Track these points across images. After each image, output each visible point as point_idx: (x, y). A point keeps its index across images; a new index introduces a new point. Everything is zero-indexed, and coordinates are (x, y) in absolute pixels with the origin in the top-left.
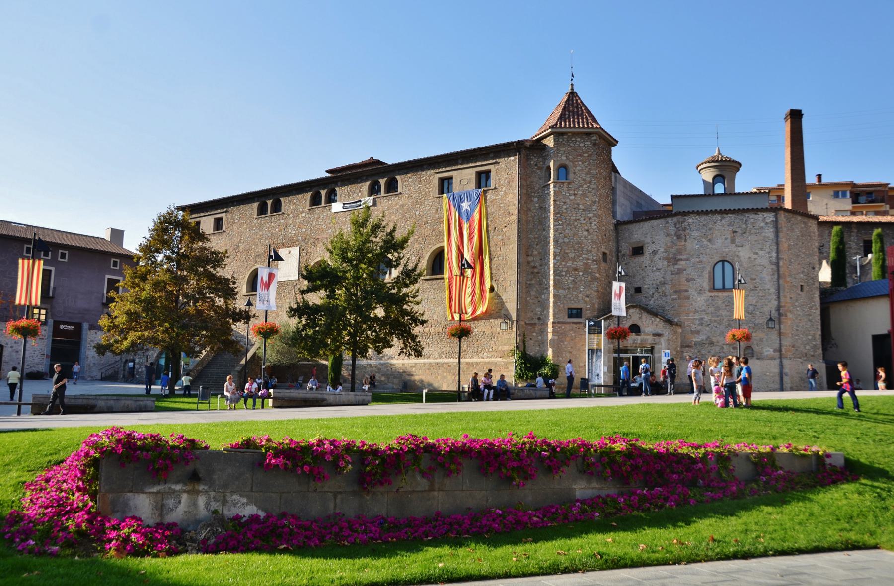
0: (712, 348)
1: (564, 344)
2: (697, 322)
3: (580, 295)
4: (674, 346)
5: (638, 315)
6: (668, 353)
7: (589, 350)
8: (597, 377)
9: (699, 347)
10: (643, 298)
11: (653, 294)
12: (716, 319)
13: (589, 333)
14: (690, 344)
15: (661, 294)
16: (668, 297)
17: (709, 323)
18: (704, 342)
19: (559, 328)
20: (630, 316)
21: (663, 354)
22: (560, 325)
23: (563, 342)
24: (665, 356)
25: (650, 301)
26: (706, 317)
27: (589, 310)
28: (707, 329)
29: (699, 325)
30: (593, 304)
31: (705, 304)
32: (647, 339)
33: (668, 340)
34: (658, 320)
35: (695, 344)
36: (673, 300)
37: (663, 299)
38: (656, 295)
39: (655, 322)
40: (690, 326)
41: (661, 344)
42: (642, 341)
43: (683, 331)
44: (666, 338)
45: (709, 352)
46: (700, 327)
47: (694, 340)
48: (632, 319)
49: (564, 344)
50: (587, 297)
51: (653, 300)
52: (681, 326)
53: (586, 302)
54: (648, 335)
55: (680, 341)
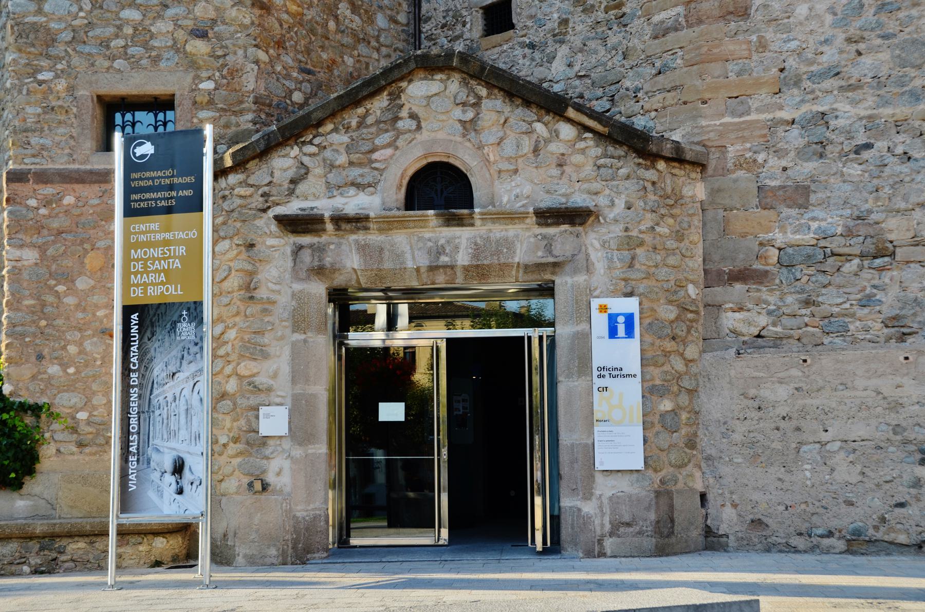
0: (886, 277)
1: (72, 290)
2: (795, 138)
3: (162, 27)
4: (663, 273)
5: (458, 113)
6: (629, 319)
7: (128, 311)
8: (170, 479)
9: (803, 272)
10: (519, 52)
11: (564, 22)
12: (900, 110)
13: (130, 212)
14: (757, 266)
15: (601, 15)
16: (636, 24)
17: (861, 139)
18: (835, 245)
19: (47, 203)
20: (413, 116)
21: (600, 323)
22: (48, 190)
23: (68, 278)
24: (613, 333)
25: (551, 59)
26: (843, 107)
27: (211, 103)
28: (854, 170)
29: (802, 154)
30: (234, 73)
31: (841, 37)
32: (509, 244)
33: (630, 243)
34: (567, 131)
35: (786, 264)
36: (661, 32)
37: (613, 40)
38: (580, 25)
39: (555, 148)
40: (751, 165)
41: (589, 269)
42: (477, 251)
43: (714, 192)
44: (617, 230)
45: (867, 302)
46: (810, 167)
47: (780, 238)
48: (424, 136)
49: (72, 290)
50: (201, 34)
51: (563, 51)
52: (700, 165)
53: (192, 64)
54: (511, 217)
55: (699, 251)
